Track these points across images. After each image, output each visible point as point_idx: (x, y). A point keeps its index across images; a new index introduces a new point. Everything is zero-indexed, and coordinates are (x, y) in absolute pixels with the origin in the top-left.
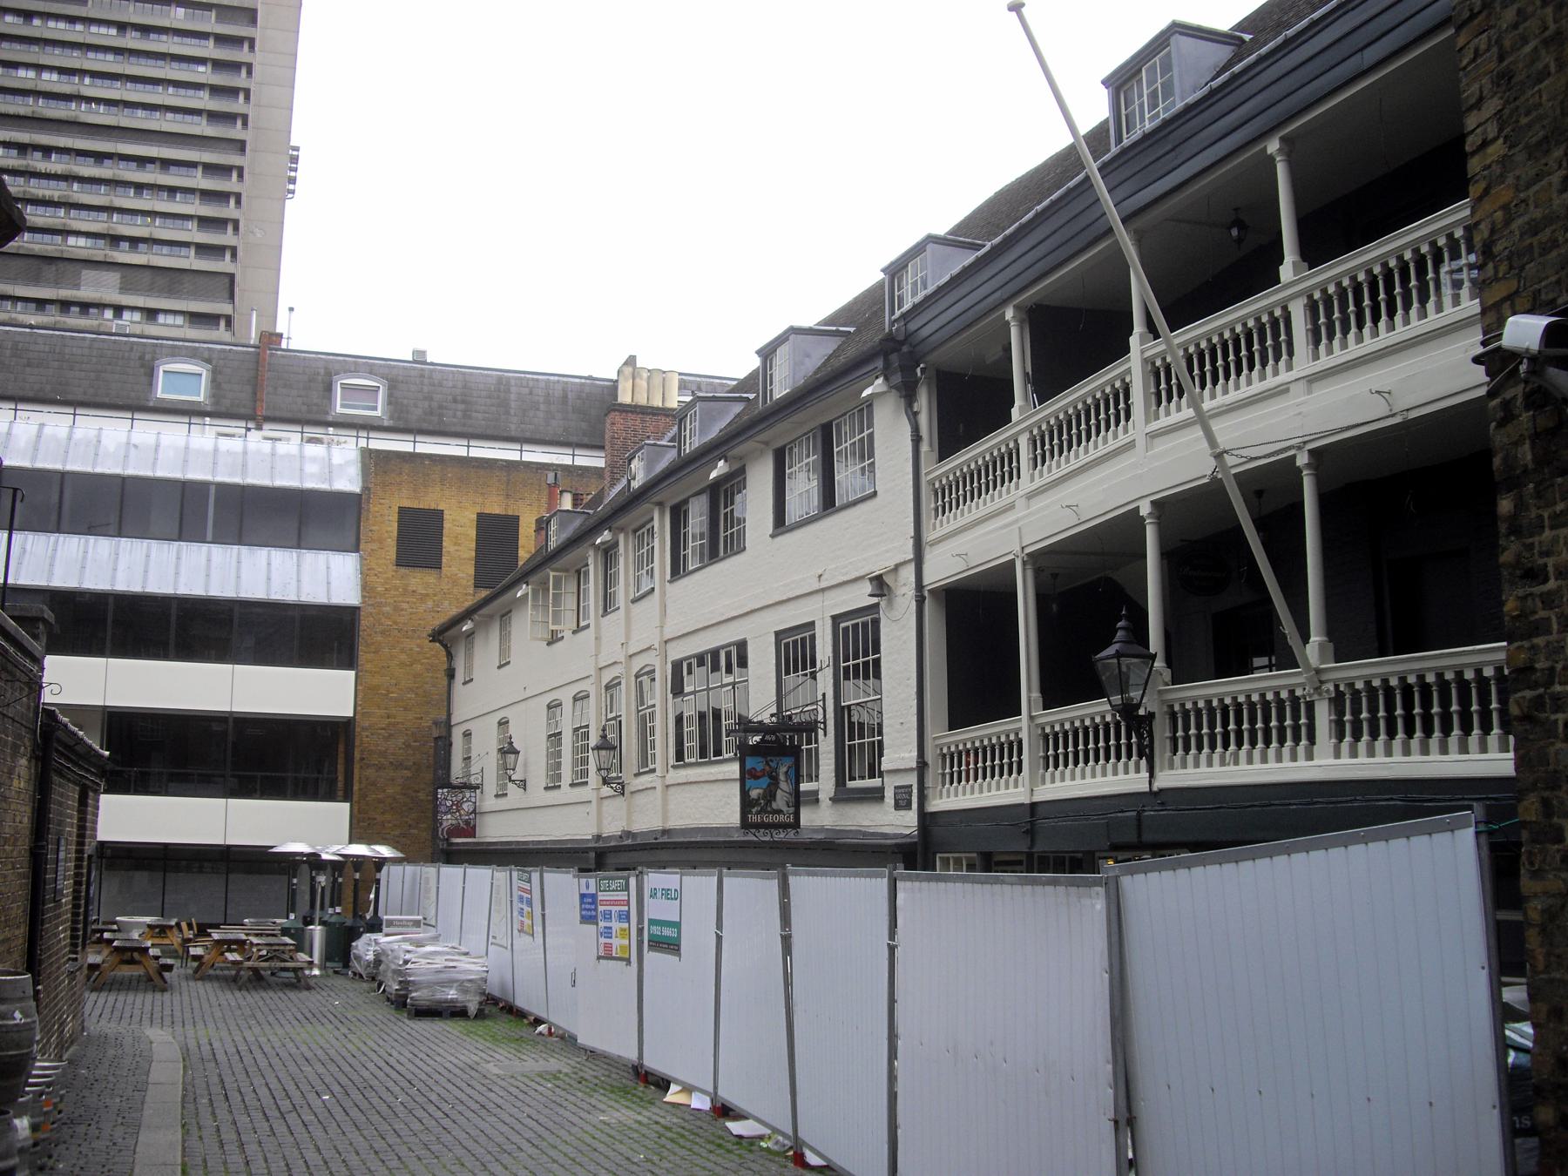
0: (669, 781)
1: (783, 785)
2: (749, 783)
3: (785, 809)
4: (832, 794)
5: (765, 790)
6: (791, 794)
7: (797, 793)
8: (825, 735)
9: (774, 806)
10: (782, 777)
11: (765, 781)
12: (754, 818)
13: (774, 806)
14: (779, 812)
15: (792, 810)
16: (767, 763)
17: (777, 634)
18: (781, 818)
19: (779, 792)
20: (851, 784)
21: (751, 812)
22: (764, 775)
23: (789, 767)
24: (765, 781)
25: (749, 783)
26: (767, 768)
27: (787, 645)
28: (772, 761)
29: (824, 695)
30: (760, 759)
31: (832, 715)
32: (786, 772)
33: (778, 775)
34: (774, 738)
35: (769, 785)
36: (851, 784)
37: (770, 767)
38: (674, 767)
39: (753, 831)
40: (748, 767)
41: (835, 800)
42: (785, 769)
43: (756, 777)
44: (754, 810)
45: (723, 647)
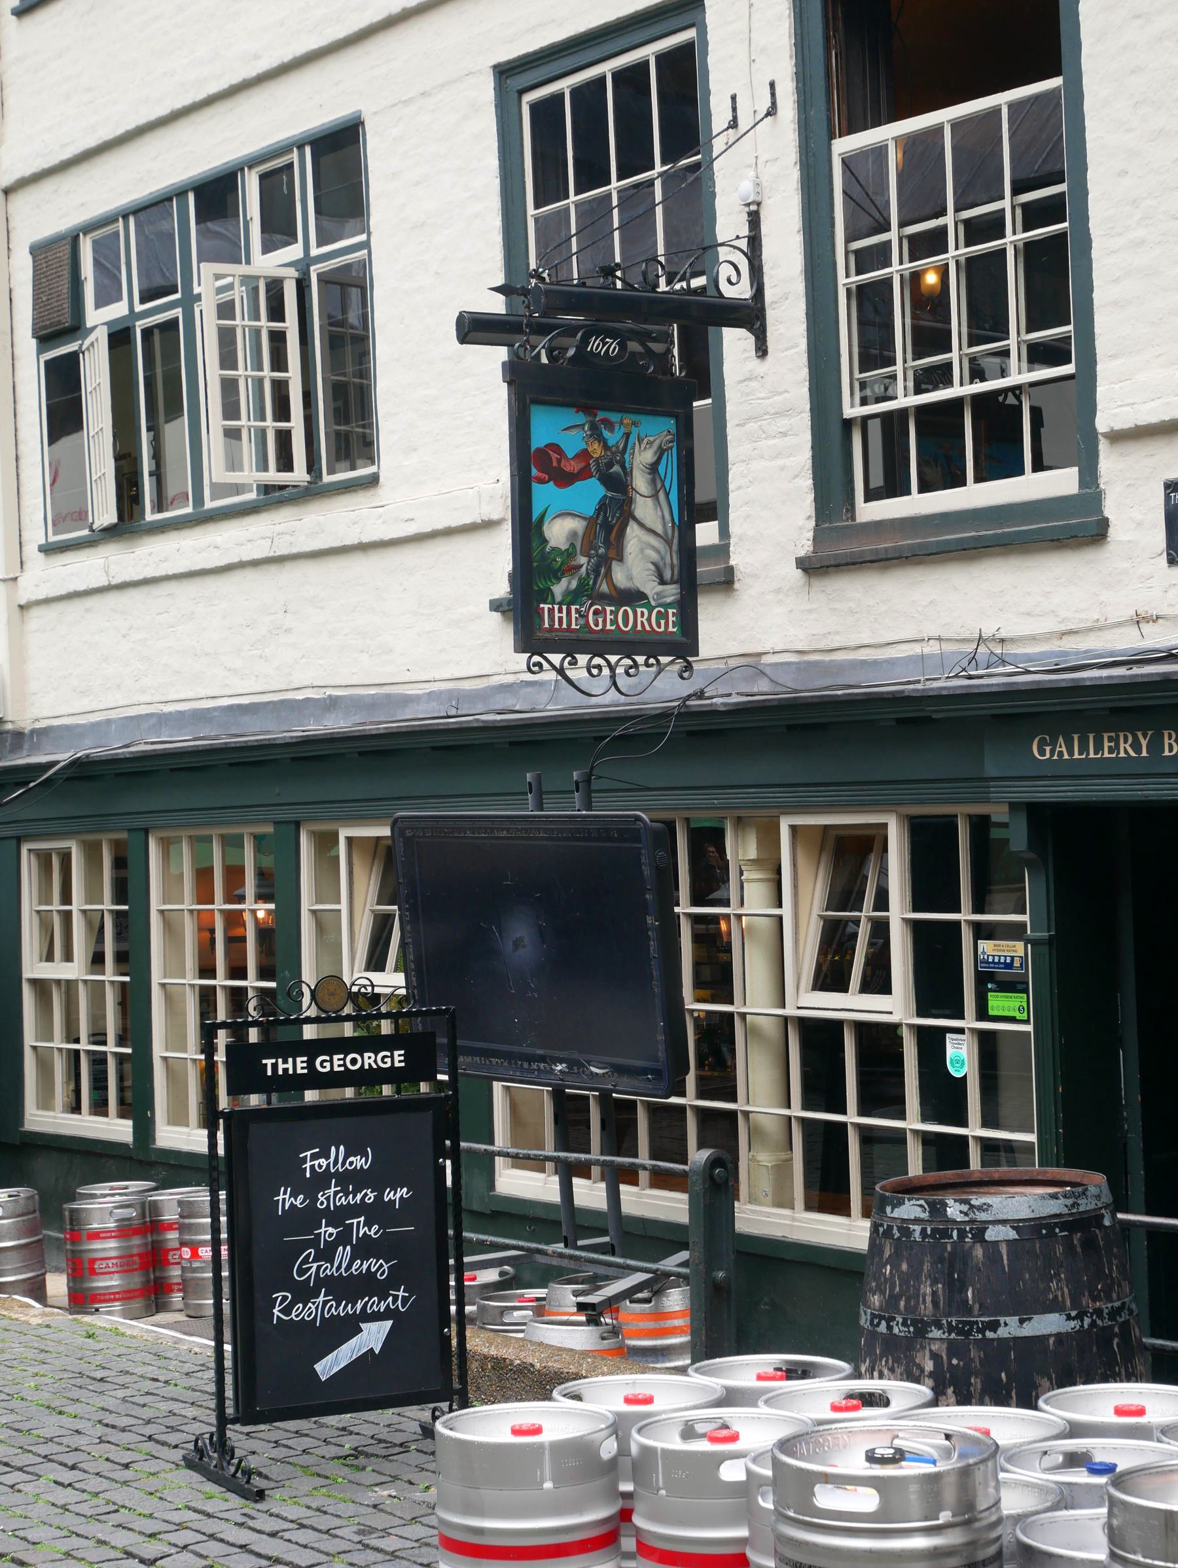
0: (29, 589)
1: (644, 509)
2: (544, 495)
3: (651, 587)
4: (805, 546)
5: (591, 521)
6: (669, 543)
7: (688, 552)
8: (762, 350)
9: (620, 576)
10: (640, 482)
11: (589, 494)
12: (560, 614)
13: (620, 576)
14: (633, 597)
15: (672, 592)
16: (595, 433)
17: (504, 72)
18: (640, 619)
19: (632, 530)
20: (870, 511)
21: (546, 595)
22: (584, 474)
23: (661, 452)
24: (589, 494)
25: (544, 495)
26: (596, 450)
27: (546, 112)
28: (610, 426)
29: (754, 220)
30: (581, 418)
31: (799, 287)
32: (653, 468)
33: (628, 473)
34: (613, 347)
35: (602, 506)
36: (870, 511)
37: (606, 447)
38: (48, 550)
39: (556, 658)
40: (540, 438)
41: (812, 567)
42: (646, 456)
43: (564, 479)
44: (558, 589)
45: (253, 162)
